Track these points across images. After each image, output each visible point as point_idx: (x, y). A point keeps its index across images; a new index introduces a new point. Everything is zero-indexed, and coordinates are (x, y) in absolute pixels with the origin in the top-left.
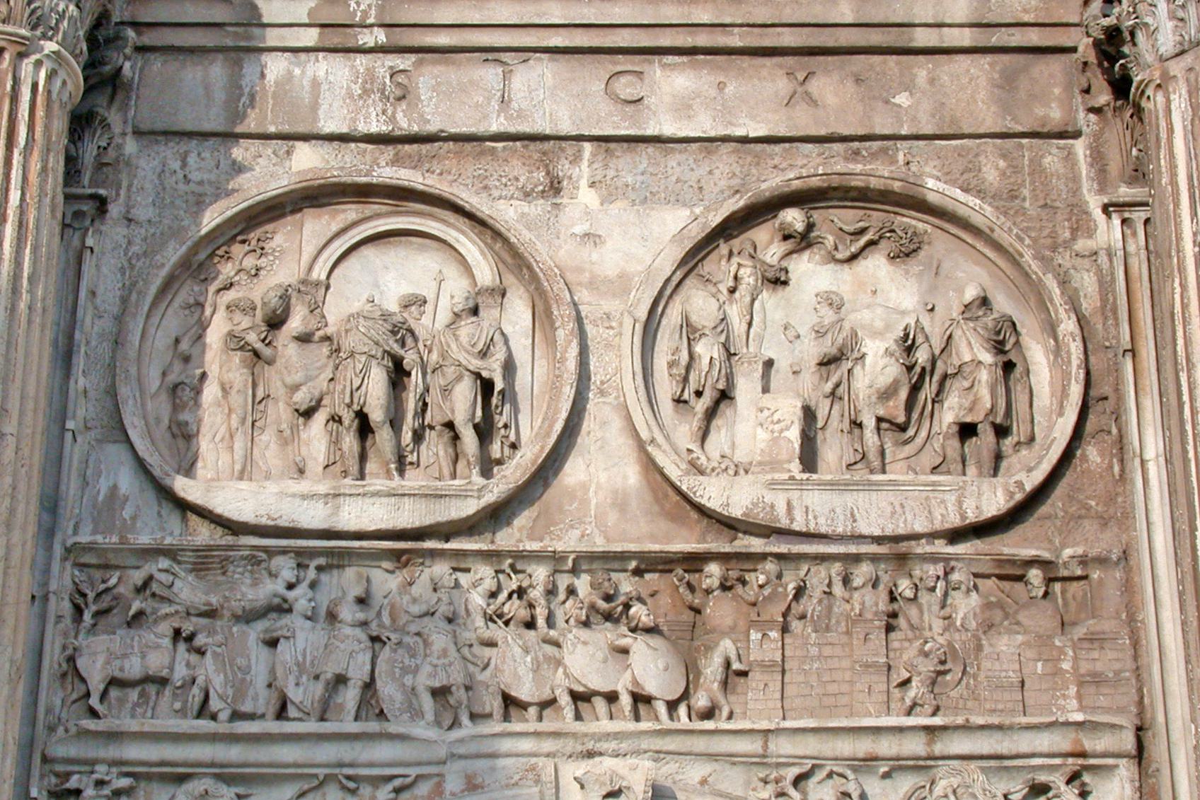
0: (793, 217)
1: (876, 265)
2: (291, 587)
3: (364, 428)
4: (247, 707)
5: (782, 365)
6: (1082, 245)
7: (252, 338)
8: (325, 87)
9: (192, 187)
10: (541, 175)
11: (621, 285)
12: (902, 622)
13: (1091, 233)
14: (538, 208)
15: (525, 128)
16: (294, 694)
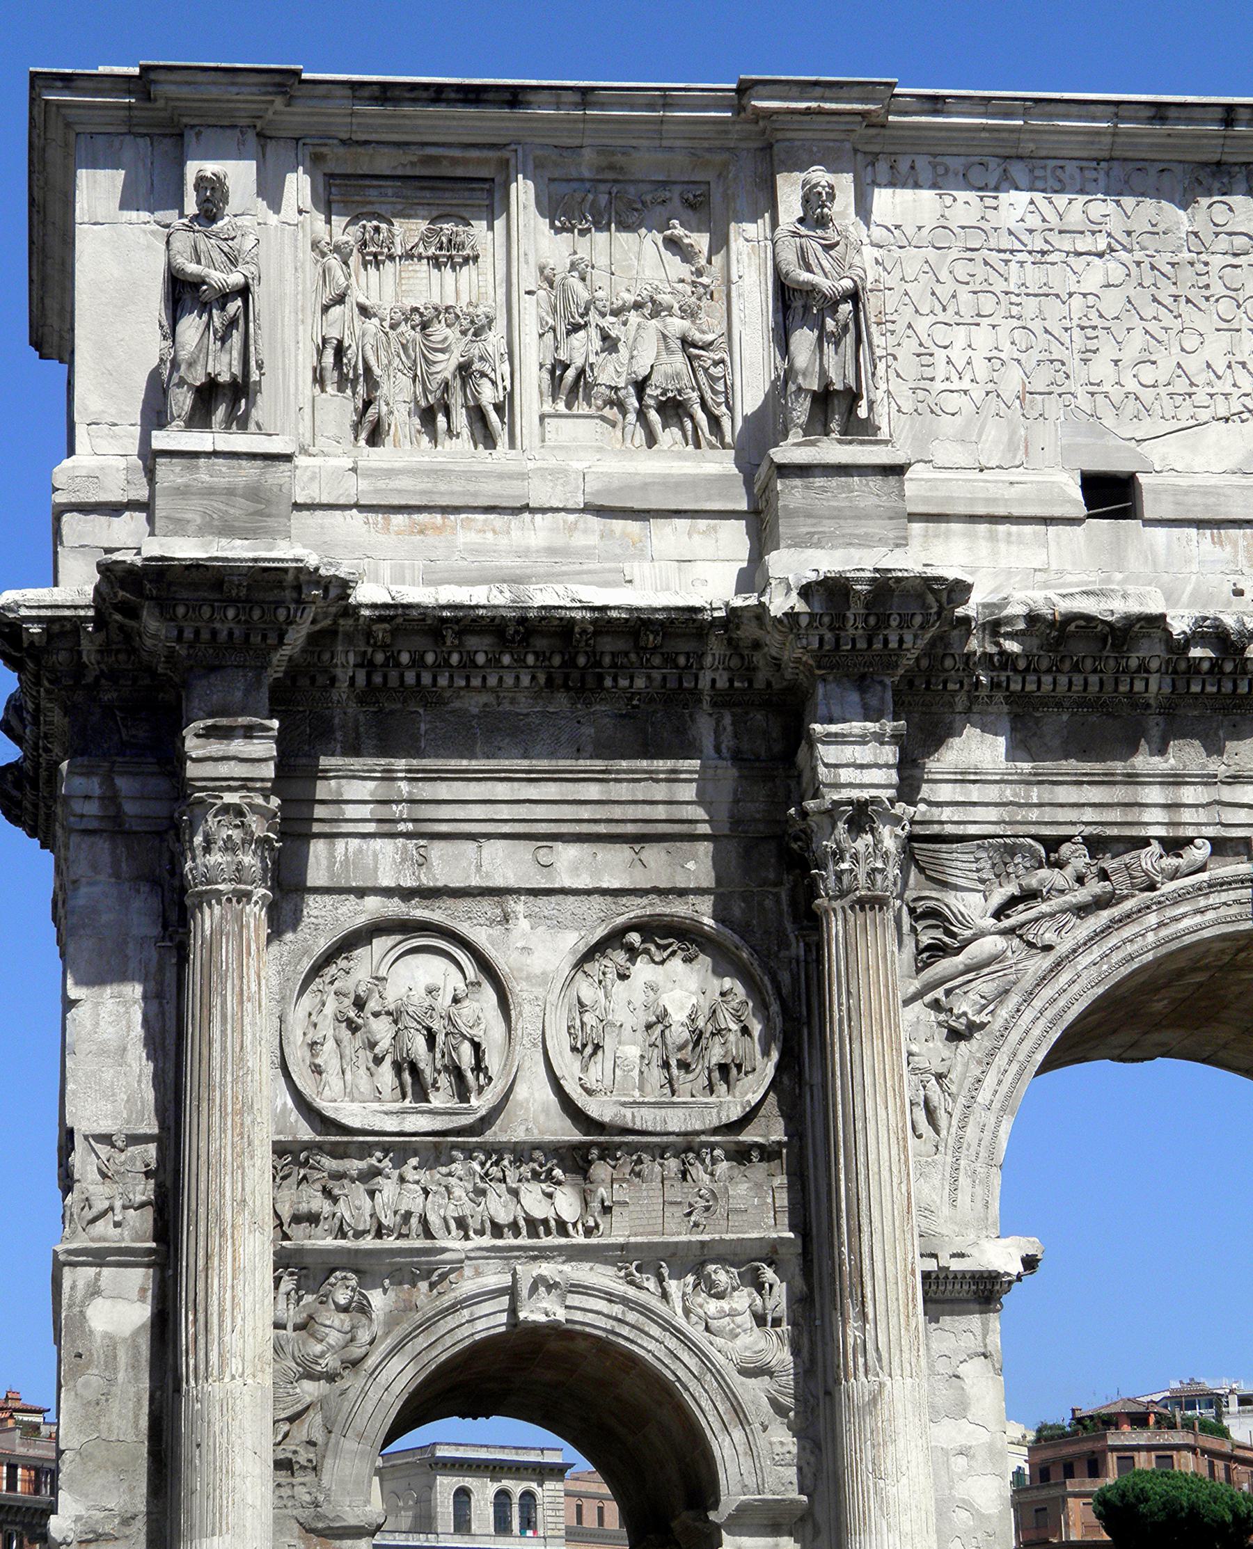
0: (634, 938)
1: (676, 963)
2: (380, 1161)
3: (414, 1069)
4: (361, 1228)
5: (627, 1027)
6: (783, 954)
7: (352, 1014)
8: (380, 856)
9: (313, 920)
10: (498, 911)
11: (544, 979)
12: (688, 1177)
13: (788, 947)
14: (497, 930)
15: (490, 884)
16: (385, 1222)
